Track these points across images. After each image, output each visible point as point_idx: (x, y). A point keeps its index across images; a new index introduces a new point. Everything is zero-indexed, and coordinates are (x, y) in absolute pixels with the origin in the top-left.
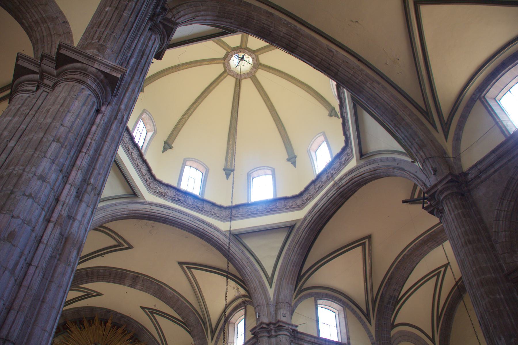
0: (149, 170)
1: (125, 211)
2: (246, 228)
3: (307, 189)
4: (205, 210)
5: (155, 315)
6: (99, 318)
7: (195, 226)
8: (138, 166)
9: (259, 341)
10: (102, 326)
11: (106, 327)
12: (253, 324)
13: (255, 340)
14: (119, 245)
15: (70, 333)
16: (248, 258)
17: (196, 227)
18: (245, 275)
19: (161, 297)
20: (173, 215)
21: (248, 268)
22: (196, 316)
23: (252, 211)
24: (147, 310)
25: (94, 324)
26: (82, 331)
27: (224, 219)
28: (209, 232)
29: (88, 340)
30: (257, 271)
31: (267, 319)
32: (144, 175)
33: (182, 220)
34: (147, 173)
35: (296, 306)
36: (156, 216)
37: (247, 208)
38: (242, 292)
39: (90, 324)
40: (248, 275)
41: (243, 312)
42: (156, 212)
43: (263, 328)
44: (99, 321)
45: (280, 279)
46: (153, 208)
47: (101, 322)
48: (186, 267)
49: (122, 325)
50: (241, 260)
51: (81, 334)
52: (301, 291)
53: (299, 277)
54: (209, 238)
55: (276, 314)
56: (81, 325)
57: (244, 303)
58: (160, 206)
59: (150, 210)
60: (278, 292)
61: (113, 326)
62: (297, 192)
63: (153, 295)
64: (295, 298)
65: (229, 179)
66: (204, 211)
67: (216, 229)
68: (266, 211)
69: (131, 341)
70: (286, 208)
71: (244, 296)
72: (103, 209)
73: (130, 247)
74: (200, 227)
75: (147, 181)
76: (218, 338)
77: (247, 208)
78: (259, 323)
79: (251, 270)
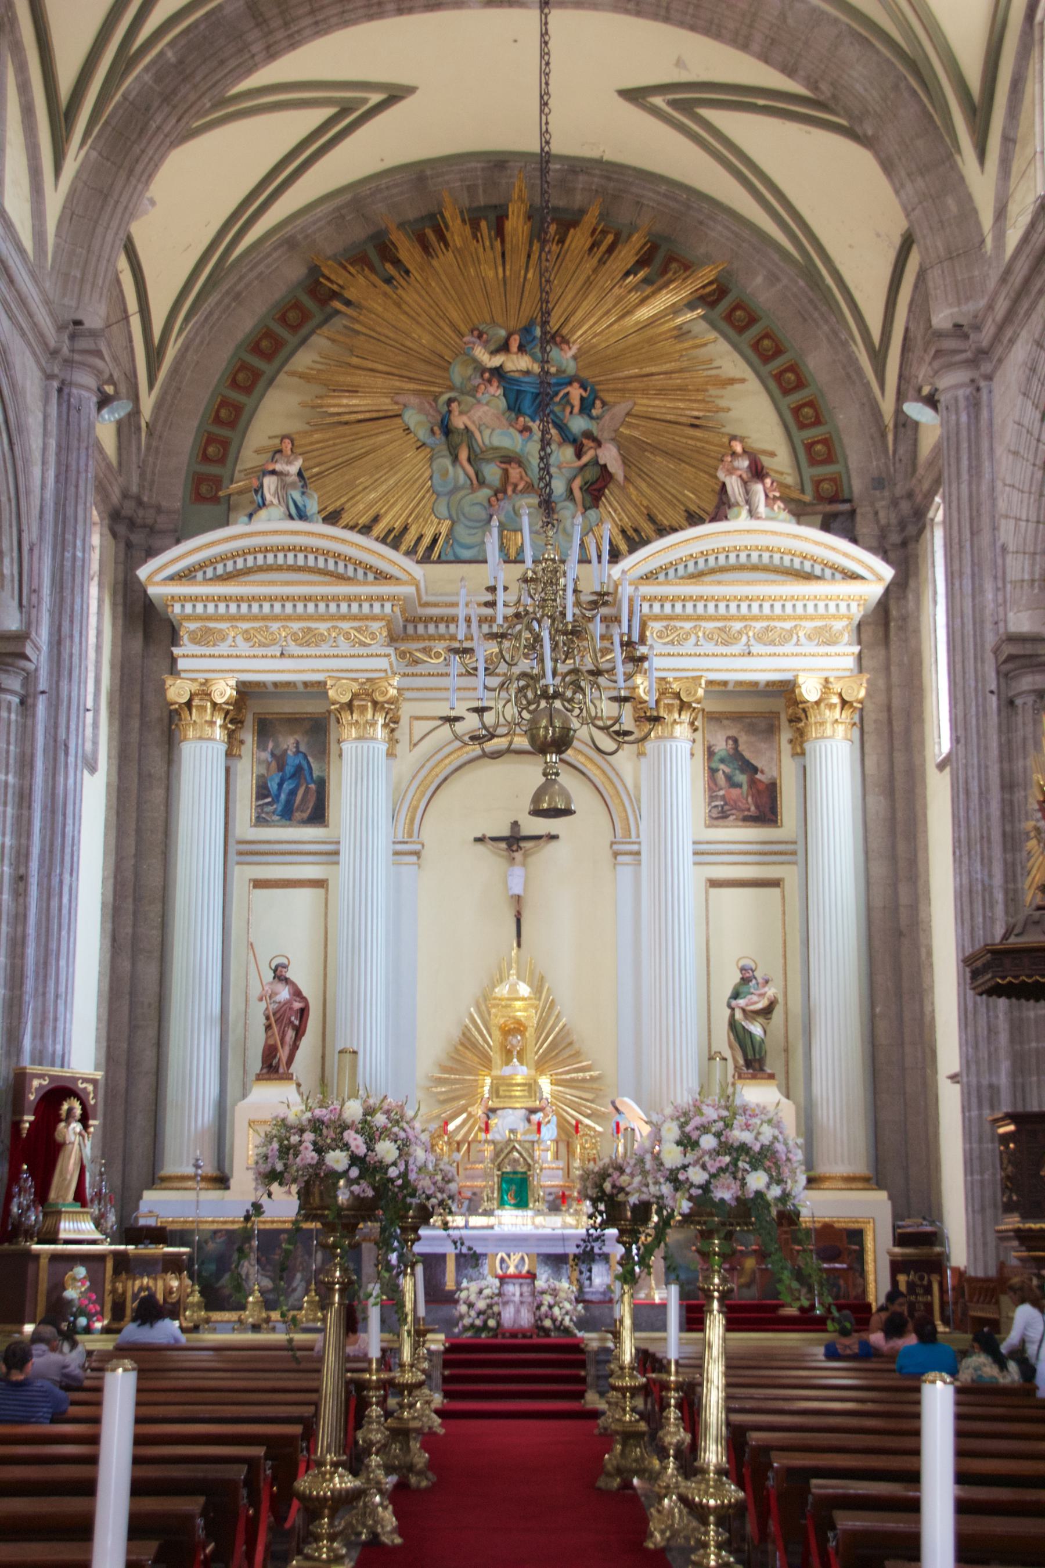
5: (709, 114)
6: (462, 212)
10: (487, 243)
11: (508, 239)
15: (355, 314)
19: (668, 9)
22: (878, 52)
25: (447, 245)
26: (400, 291)
29: (442, 324)
39: (426, 248)
44: (464, 221)
47: (475, 227)
49: (582, 212)
51: (399, 306)
56: (388, 266)
61: (538, 234)
63: (627, 12)
69: (641, 275)
76: (1009, 140)
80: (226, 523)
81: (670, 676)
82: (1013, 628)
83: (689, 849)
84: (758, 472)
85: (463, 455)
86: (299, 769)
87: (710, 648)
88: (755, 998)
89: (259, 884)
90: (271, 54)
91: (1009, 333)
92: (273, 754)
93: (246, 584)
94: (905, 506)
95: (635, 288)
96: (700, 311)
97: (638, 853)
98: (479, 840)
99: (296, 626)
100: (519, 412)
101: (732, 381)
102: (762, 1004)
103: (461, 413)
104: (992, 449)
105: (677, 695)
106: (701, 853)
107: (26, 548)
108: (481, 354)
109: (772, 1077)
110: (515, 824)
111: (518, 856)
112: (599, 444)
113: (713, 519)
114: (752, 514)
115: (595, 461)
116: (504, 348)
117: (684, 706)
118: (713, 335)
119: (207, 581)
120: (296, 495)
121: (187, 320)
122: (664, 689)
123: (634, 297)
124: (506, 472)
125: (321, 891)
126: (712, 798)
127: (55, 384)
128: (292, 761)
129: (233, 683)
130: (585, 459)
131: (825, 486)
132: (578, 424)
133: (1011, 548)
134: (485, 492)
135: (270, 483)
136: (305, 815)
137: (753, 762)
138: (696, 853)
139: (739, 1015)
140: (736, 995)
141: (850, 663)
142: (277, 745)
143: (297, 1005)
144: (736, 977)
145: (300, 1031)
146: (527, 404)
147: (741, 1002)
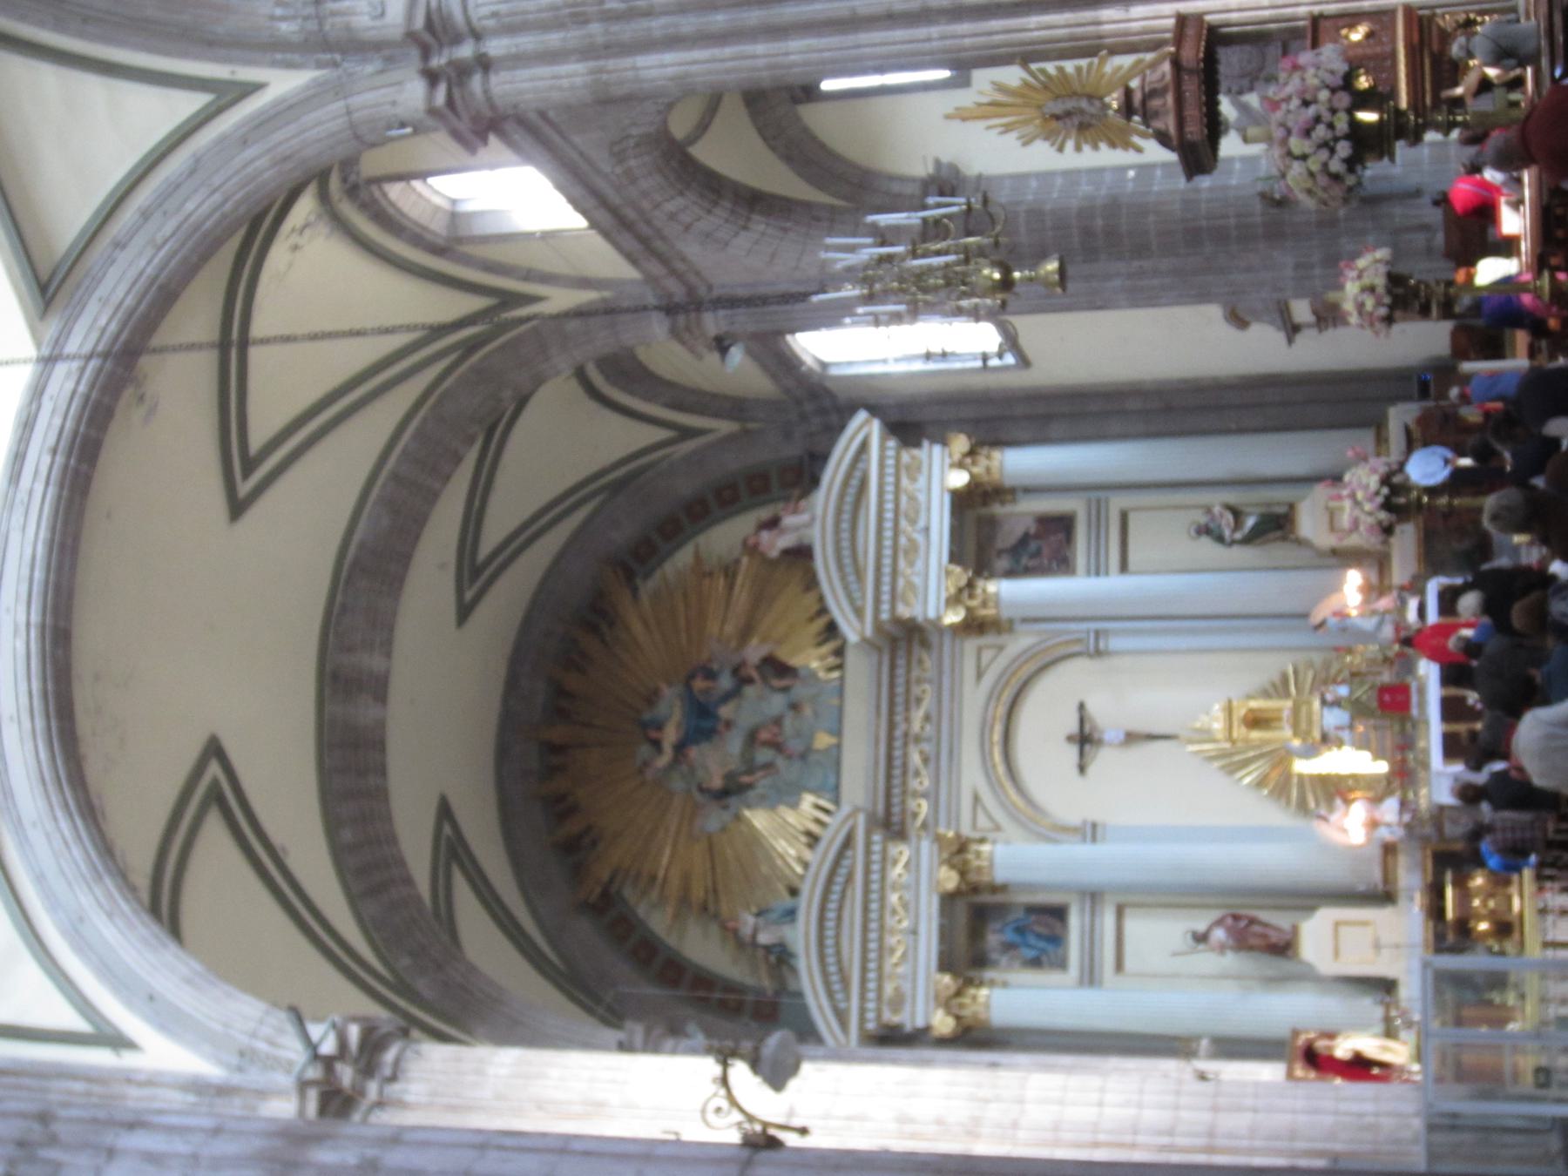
1: (59, 830)
9: (510, 112)
12: (439, 144)
13: (509, 126)
14: (215, 797)
16: (146, 215)
18: (224, 216)
20: (22, 608)
21: (190, 206)
24: (469, 595)
28: (58, 421)
30: (197, 163)
31: (409, 86)
38: (305, 207)
39: (572, 810)
40: (225, 201)
41: (395, 191)
42: (23, 687)
43: (450, 102)
50: (159, 248)
54: (86, 414)
57: (352, 191)
71: (324, 197)
72: (77, 931)
73: (214, 750)
76: (529, 275)
78: (430, 122)
79: (196, 191)
80: (799, 994)
81: (944, 595)
86: (1020, 930)
87: (919, 565)
88: (1224, 522)
89: (1119, 965)
90: (408, 881)
91: (680, 266)
93: (851, 960)
94: (809, 407)
97: (1097, 633)
98: (1082, 769)
102: (1229, 517)
105: (960, 590)
106: (1098, 570)
108: (664, 760)
109: (1292, 506)
110: (1070, 739)
111: (1096, 736)
112: (743, 664)
115: (758, 668)
116: (657, 745)
117: (970, 585)
118: (658, 574)
119: (848, 999)
120: (773, 916)
122: (954, 601)
125: (1128, 912)
128: (1010, 936)
129: (938, 976)
130: (755, 674)
132: (725, 682)
134: (781, 762)
135: (764, 938)
136: (1058, 924)
138: (1098, 574)
139: (1238, 536)
140: (1220, 539)
143: (1229, 921)
144: (1206, 543)
145: (1252, 921)
146: (706, 724)
147: (1227, 533)
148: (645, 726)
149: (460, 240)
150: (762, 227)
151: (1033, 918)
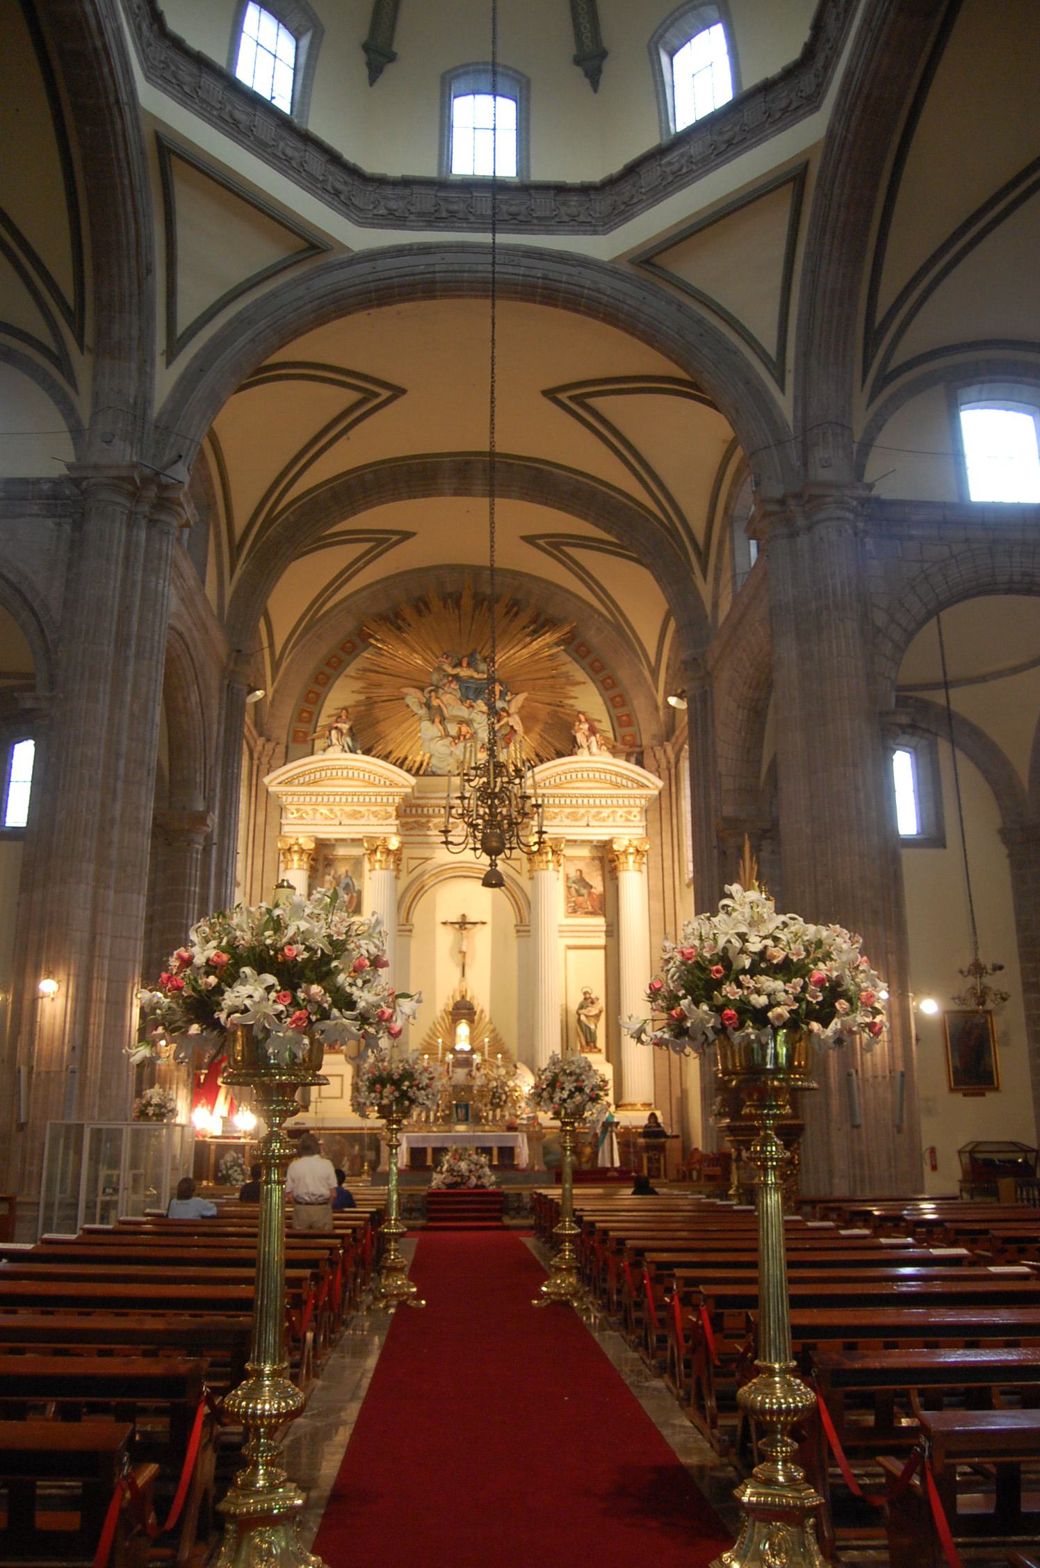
0: (334, 158)
2: (667, 230)
3: (818, 27)
4: (537, 218)
7: (519, 275)
8: (289, 159)
16: (700, 321)
17: (521, 278)
20: (444, 267)
23: (675, 167)
24: (541, 542)
27: (605, 224)
28: (564, 278)
30: (736, 352)
32: (321, 178)
33: (477, 272)
34: (332, 168)
35: (876, 426)
36: (399, 286)
37: (660, 165)
39: (420, 613)
42: (393, 273)
45: (804, 354)
46: (381, 264)
48: (570, 398)
52: (885, 379)
53: (872, 337)
55: (805, 464)
56: (399, 621)
58: (399, 251)
59: (375, 276)
60: (802, 401)
62: (794, 54)
64: (871, 401)
65: (601, 88)
66: (535, 221)
67: (584, 262)
68: (715, 153)
69: (531, 628)
70: (770, 120)
73: (398, 392)
74: (533, 272)
75: (337, 193)
76: (718, 570)
77: (660, 165)
82: (725, 814)
83: (557, 929)
84: (593, 731)
85: (437, 720)
87: (567, 822)
92: (334, 878)
95: (528, 635)
96: (562, 647)
99: (347, 809)
100: (468, 698)
101: (578, 683)
102: (597, 1012)
103: (437, 698)
104: (713, 721)
107: (208, 767)
110: (464, 916)
113: (569, 755)
114: (591, 753)
115: (507, 724)
116: (459, 664)
121: (293, 647)
123: (528, 639)
124: (460, 729)
126: (569, 902)
127: (226, 682)
131: (628, 738)
133: (724, 773)
137: (591, 883)
139: (583, 1018)
140: (582, 1007)
141: (641, 831)
142: (336, 872)
144: (581, 998)
148: (472, 655)
149: (731, 525)
150: (740, 717)
151: (355, 895)
